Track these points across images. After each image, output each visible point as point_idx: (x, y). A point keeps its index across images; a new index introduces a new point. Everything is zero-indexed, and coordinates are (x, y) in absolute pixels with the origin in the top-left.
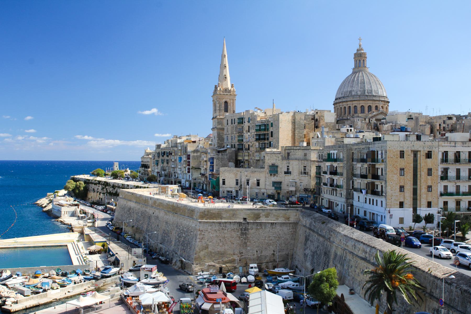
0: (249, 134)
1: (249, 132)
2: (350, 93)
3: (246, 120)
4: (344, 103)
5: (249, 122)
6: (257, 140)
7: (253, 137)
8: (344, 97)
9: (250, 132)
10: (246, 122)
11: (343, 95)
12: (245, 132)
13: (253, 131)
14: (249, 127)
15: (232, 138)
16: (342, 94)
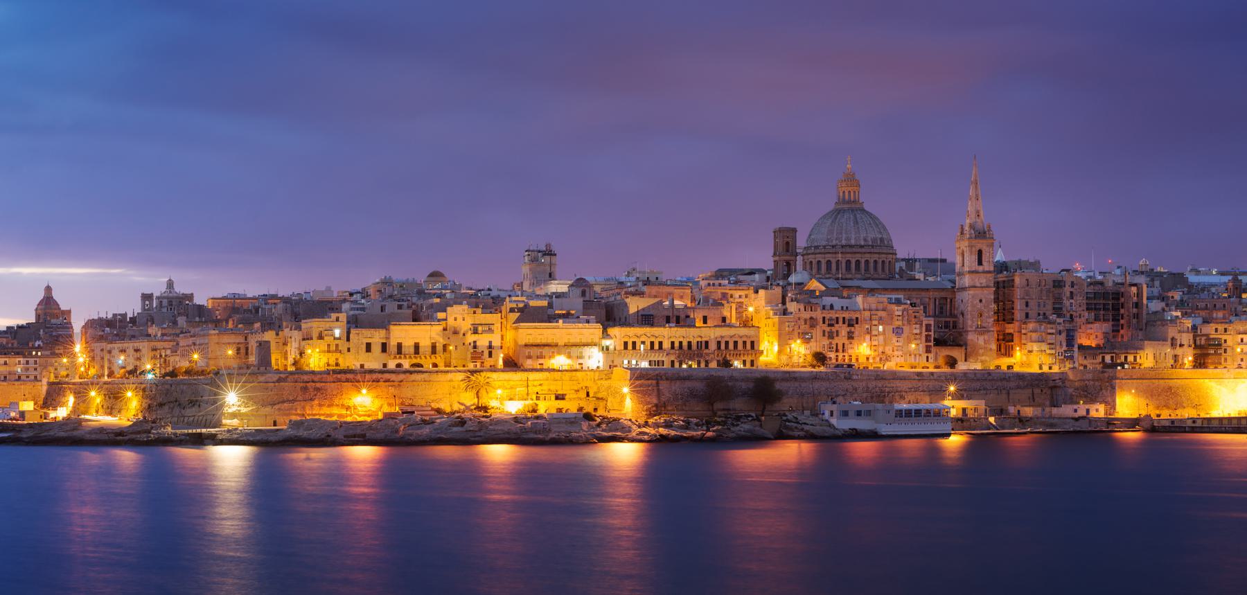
0: (1071, 301)
1: (1072, 299)
2: (881, 241)
3: (1068, 284)
4: (883, 256)
5: (1072, 287)
6: (1087, 309)
7: (1080, 306)
8: (873, 246)
9: (1075, 298)
10: (1067, 286)
11: (870, 243)
12: (1064, 298)
13: (1080, 300)
14: (1071, 293)
15: (1039, 306)
16: (865, 240)
